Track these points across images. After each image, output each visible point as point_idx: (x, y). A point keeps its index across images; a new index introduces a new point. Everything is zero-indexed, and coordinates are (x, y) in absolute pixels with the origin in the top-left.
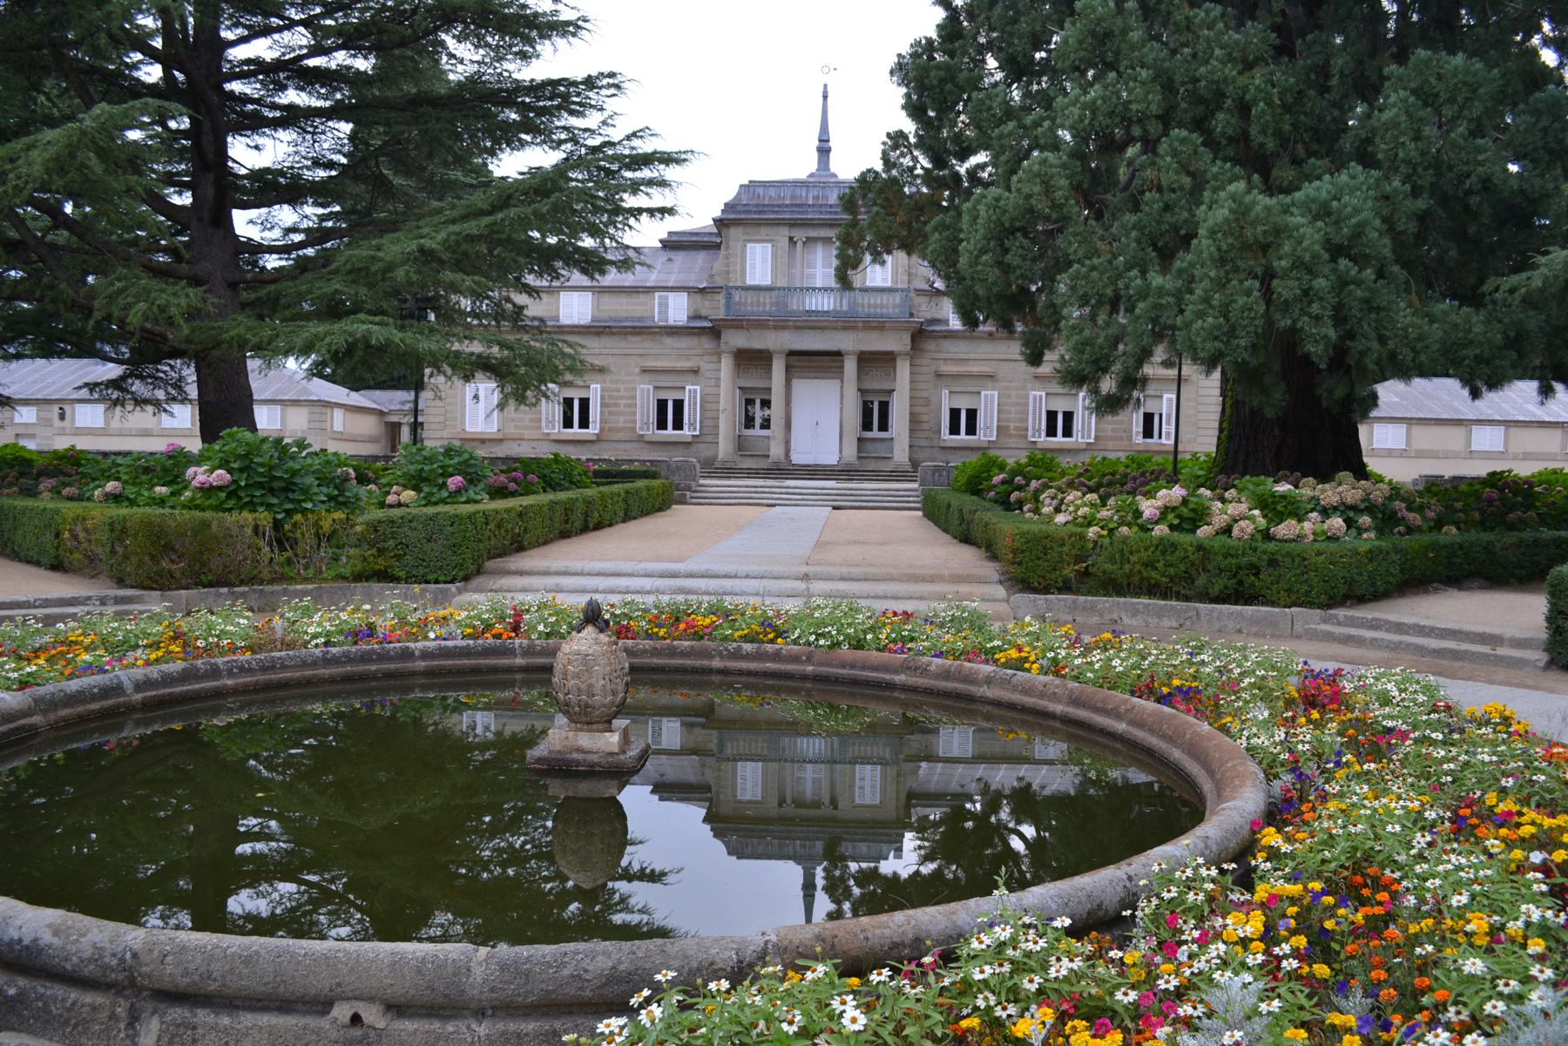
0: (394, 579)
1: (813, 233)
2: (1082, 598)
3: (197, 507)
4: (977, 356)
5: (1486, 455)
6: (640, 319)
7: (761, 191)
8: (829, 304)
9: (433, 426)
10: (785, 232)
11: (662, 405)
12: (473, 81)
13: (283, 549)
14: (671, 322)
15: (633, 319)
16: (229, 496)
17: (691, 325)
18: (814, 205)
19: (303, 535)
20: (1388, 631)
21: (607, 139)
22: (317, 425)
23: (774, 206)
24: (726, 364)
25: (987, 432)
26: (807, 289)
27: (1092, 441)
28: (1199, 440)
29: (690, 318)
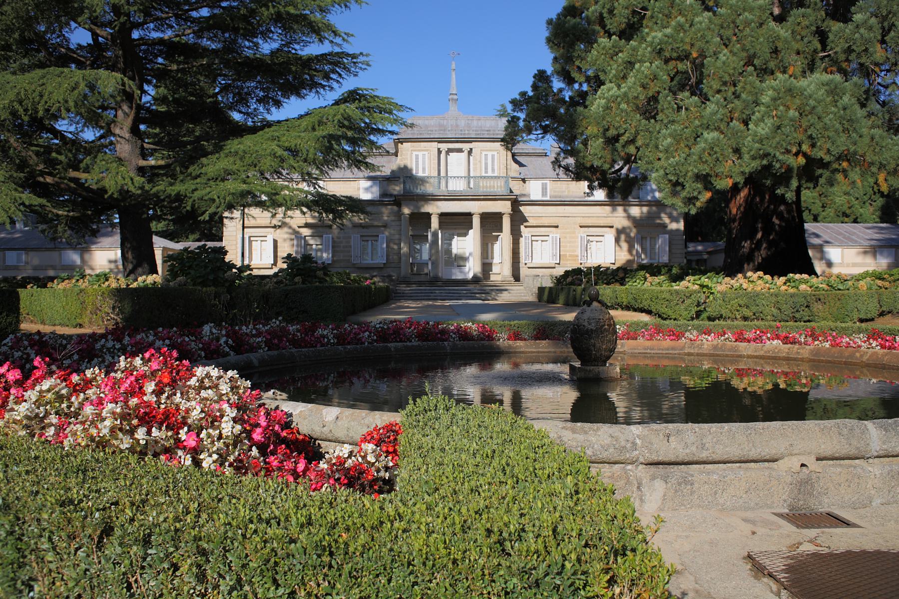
10: (435, 145)
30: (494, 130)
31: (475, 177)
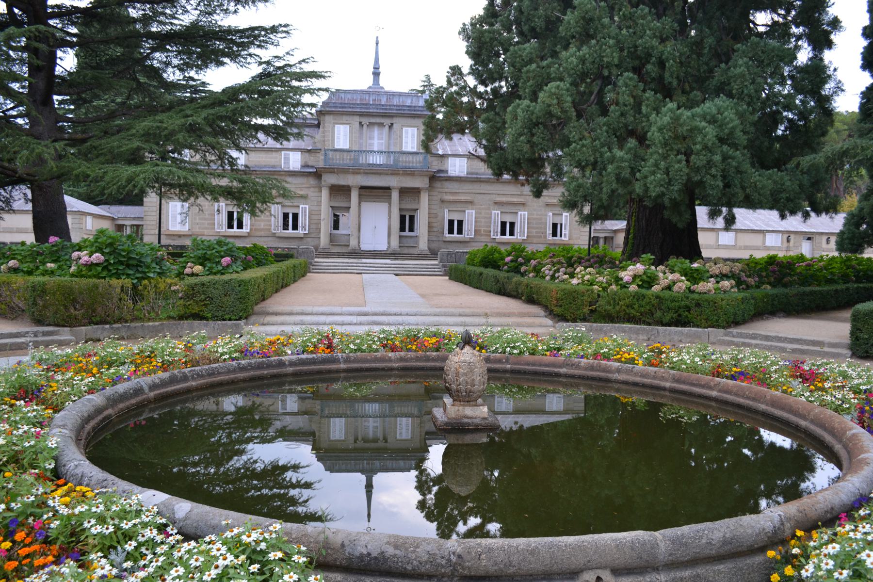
0: (206, 319)
1: (373, 120)
2: (595, 325)
3: (82, 276)
4: (463, 191)
5: (726, 247)
6: (274, 166)
7: (343, 95)
8: (380, 160)
9: (149, 227)
10: (357, 119)
11: (286, 216)
12: (195, 25)
13: (135, 302)
14: (291, 169)
15: (269, 166)
16: (102, 270)
17: (302, 170)
18: (373, 104)
19: (148, 292)
20: (761, 340)
21: (288, 63)
22: (77, 226)
23: (351, 104)
24: (325, 193)
25: (469, 232)
26: (368, 152)
27: (525, 238)
28: (581, 238)
29: (303, 167)
30: (415, 107)
31: (395, 152)
